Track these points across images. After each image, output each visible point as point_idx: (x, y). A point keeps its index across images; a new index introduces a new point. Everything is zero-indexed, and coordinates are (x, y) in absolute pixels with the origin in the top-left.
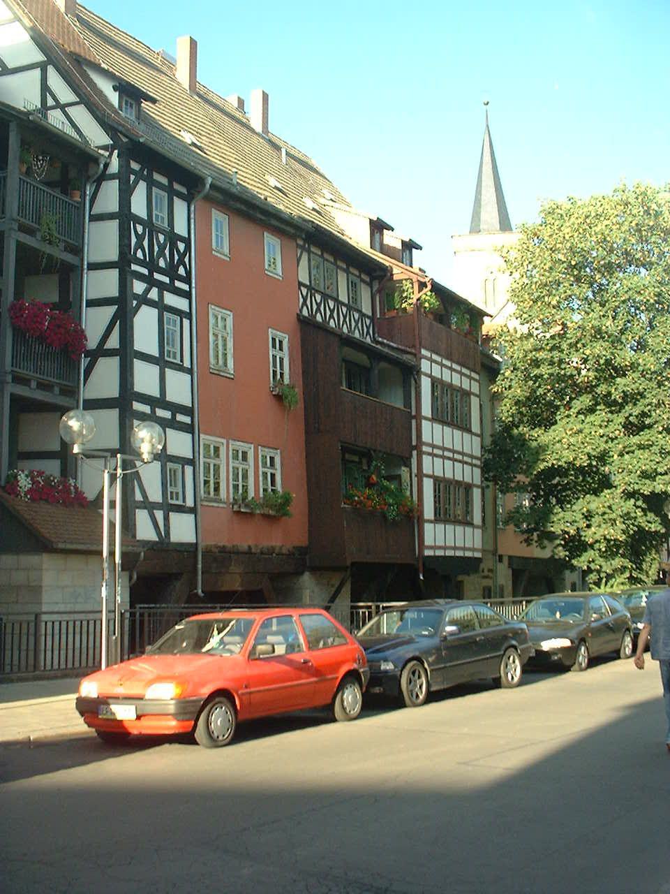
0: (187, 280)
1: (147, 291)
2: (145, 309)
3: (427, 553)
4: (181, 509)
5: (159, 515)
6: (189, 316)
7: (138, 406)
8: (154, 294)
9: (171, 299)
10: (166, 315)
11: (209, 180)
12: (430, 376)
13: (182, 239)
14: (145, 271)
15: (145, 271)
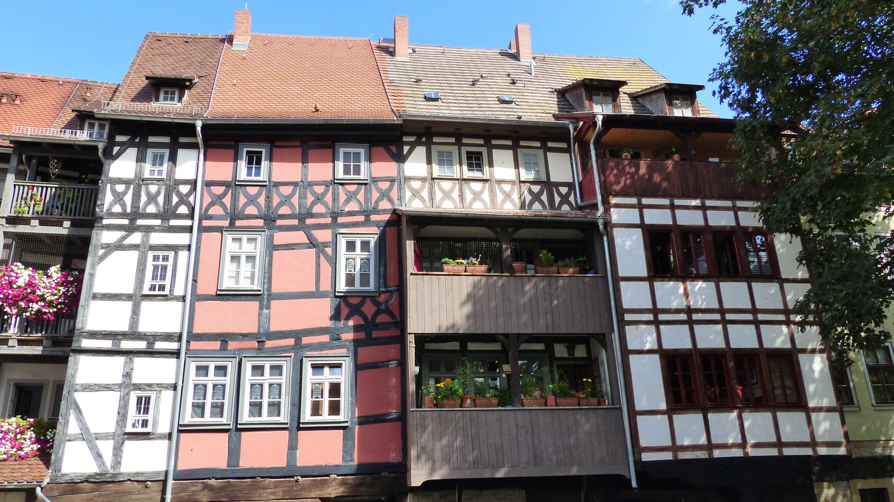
0: (191, 216)
1: (125, 238)
2: (117, 254)
3: (646, 457)
4: (145, 436)
5: (106, 448)
6: (189, 247)
7: (87, 343)
8: (136, 238)
9: (157, 238)
10: (151, 255)
11: (199, 124)
12: (642, 225)
13: (185, 182)
14: (125, 222)
15: (125, 222)
